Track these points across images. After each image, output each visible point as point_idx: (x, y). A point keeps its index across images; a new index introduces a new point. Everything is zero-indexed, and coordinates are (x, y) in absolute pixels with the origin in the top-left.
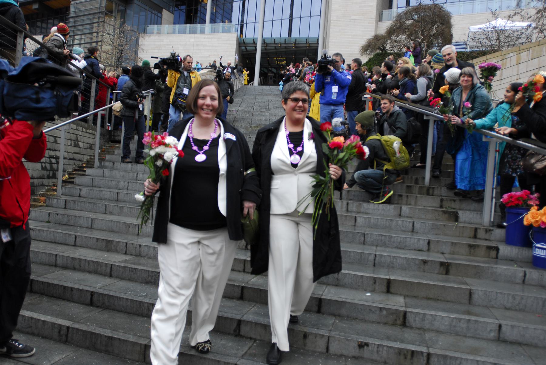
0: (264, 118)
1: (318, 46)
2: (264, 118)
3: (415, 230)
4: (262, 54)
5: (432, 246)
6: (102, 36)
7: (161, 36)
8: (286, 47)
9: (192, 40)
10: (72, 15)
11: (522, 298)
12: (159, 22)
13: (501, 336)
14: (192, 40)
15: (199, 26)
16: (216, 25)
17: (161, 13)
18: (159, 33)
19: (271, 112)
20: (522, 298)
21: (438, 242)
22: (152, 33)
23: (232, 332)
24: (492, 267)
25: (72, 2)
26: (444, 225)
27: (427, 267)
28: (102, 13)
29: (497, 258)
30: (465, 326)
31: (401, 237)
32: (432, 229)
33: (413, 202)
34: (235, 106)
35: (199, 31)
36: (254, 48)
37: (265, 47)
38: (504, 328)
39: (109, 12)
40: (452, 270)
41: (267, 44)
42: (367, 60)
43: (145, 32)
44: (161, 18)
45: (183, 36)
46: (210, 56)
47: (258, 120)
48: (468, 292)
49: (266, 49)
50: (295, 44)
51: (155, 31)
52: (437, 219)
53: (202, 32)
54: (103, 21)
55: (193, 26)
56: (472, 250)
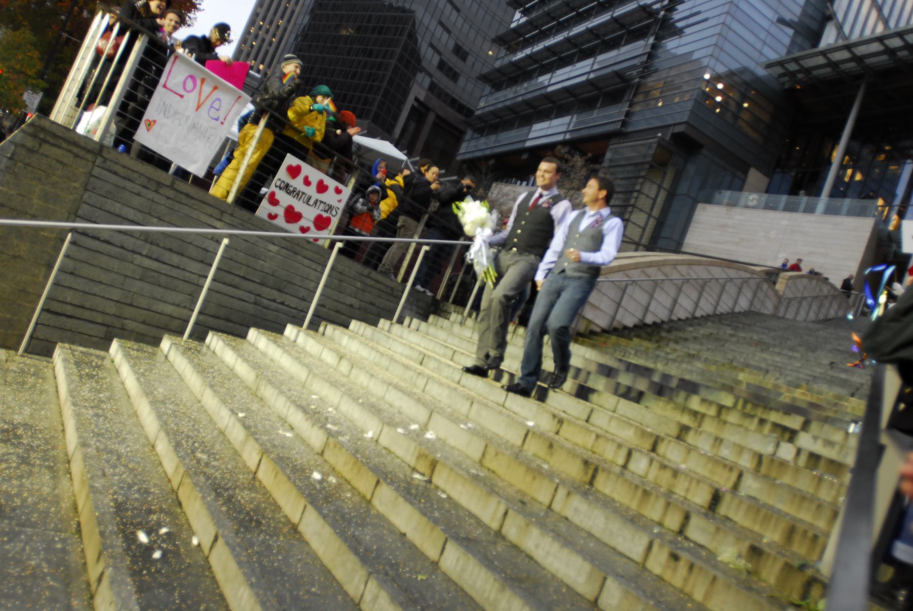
6: (637, 198)
7: (736, 210)
9: (785, 223)
10: (606, 164)
12: (738, 185)
14: (785, 223)
15: (803, 199)
16: (838, 202)
17: (746, 173)
18: (733, 204)
22: (719, 203)
25: (611, 147)
28: (647, 163)
35: (802, 206)
39: (658, 164)
43: (709, 200)
44: (744, 181)
45: (771, 214)
46: (810, 253)
51: (726, 200)
53: (810, 210)
54: (643, 177)
55: (793, 198)
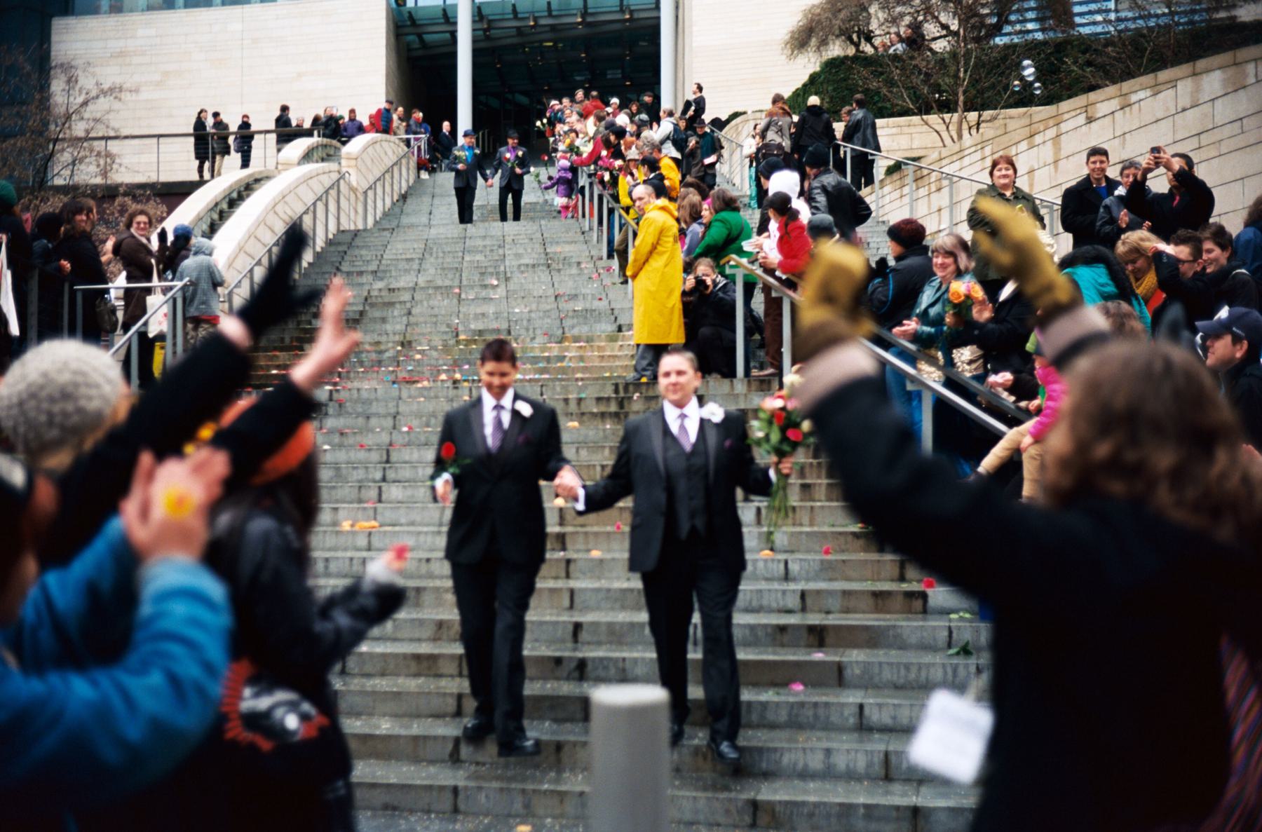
0: (491, 309)
1: (659, 18)
2: (491, 309)
3: (791, 574)
4: (477, 53)
5: (809, 601)
8: (553, 28)
11: (920, 669)
13: (865, 722)
19: (511, 286)
20: (920, 669)
21: (818, 592)
23: (447, 757)
24: (894, 626)
26: (844, 561)
27: (786, 638)
29: (925, 611)
30: (811, 713)
31: (751, 591)
32: (821, 570)
33: (806, 520)
34: (407, 271)
36: (448, 35)
37: (485, 30)
38: (867, 711)
40: (829, 639)
41: (490, 22)
42: (805, 78)
47: (476, 317)
48: (835, 668)
49: (488, 38)
50: (585, 13)
52: (843, 551)
56: (880, 602)
